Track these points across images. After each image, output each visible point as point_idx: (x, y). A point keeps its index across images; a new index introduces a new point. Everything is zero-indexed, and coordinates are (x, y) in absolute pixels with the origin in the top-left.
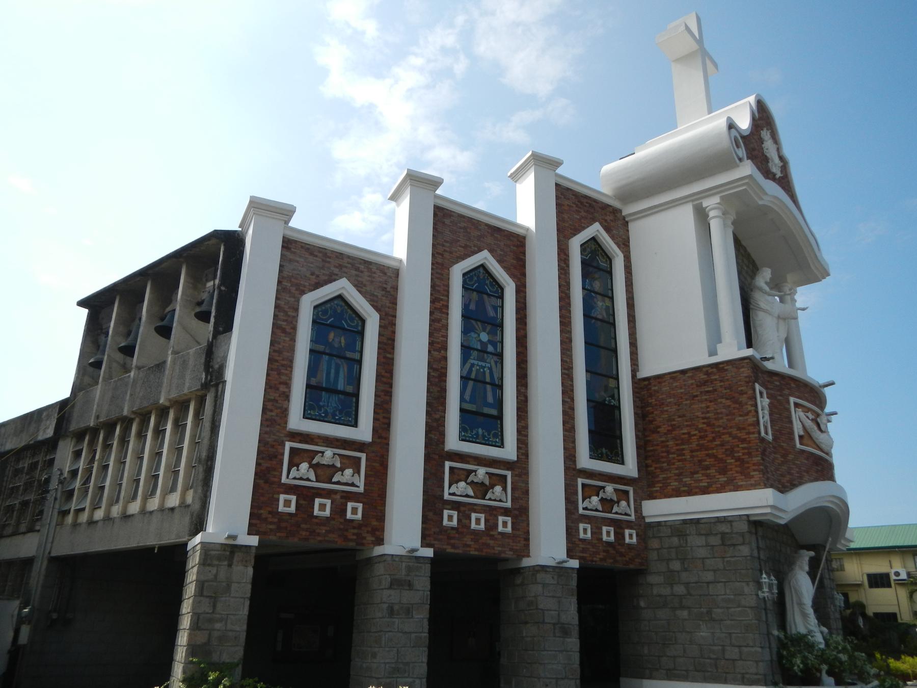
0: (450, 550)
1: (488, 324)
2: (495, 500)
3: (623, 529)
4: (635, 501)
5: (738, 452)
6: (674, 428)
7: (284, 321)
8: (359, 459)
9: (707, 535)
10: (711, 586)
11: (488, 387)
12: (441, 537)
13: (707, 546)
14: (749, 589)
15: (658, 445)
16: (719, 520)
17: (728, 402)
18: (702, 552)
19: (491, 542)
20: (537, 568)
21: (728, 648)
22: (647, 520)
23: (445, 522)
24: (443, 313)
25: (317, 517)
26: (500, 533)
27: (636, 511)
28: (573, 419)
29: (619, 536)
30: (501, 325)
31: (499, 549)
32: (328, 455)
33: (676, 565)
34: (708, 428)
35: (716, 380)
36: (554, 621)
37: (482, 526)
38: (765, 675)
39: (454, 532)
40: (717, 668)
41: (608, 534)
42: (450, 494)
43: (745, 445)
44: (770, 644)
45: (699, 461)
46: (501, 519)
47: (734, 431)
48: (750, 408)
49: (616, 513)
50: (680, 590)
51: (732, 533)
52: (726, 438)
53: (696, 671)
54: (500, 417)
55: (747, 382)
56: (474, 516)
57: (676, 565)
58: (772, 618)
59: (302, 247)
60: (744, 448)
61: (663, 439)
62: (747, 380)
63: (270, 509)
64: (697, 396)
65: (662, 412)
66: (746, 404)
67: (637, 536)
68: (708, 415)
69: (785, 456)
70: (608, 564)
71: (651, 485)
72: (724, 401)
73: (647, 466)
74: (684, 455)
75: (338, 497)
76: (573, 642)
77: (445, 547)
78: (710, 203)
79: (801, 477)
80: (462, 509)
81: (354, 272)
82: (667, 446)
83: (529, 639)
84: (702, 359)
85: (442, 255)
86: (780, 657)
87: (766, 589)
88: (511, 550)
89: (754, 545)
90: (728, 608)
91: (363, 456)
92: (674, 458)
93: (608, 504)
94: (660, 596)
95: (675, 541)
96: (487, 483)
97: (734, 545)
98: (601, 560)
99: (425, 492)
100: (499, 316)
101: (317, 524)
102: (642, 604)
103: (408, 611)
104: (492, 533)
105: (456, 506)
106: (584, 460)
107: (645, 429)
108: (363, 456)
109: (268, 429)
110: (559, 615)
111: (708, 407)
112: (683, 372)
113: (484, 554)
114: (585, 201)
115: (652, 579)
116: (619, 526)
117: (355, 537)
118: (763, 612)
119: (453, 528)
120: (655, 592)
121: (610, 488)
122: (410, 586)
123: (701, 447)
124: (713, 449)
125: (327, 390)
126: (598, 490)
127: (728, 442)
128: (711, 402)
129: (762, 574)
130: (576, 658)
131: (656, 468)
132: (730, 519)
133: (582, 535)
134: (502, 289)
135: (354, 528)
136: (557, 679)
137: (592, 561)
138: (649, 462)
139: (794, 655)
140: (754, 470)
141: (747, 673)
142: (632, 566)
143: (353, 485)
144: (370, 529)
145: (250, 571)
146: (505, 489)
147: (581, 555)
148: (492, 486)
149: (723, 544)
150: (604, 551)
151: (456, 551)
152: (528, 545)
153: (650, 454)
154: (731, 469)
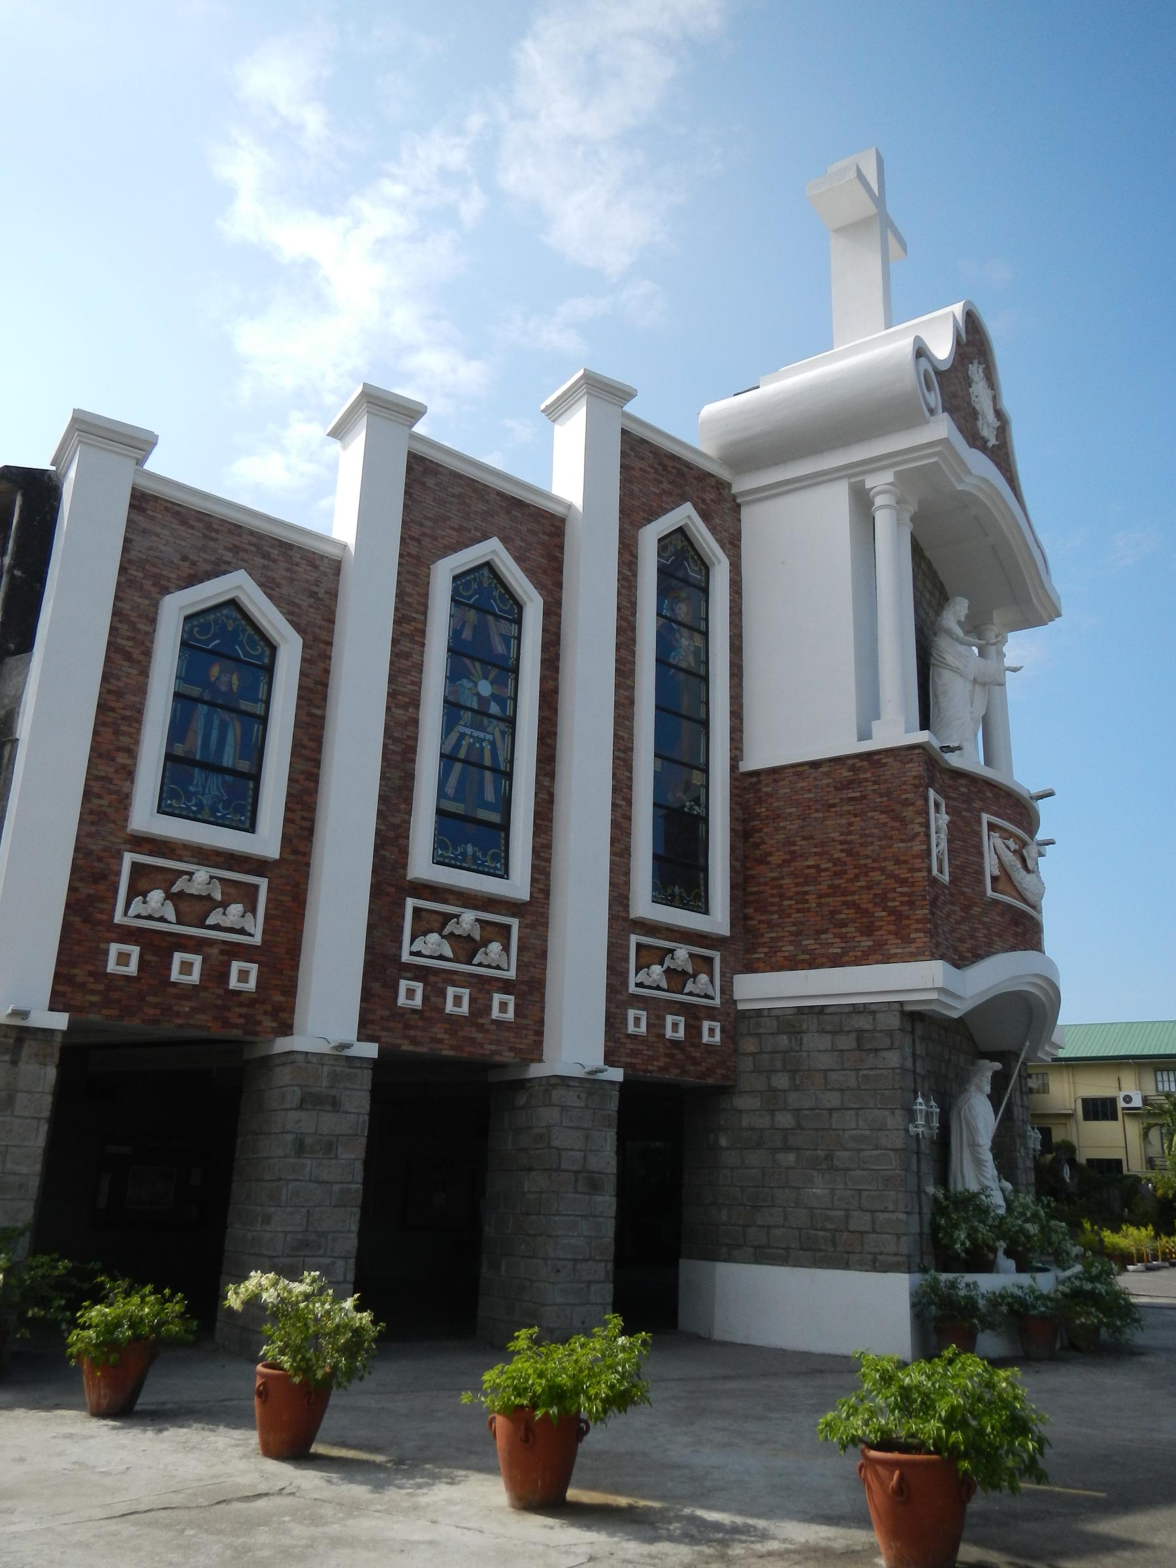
0: (406, 1047)
1: (494, 665)
2: (489, 966)
3: (699, 1019)
4: (723, 974)
5: (894, 900)
6: (793, 856)
7: (129, 639)
8: (256, 888)
9: (834, 1033)
10: (835, 1115)
11: (488, 775)
12: (392, 1024)
13: (833, 1050)
14: (895, 1120)
15: (765, 884)
16: (856, 1010)
17: (883, 818)
18: (825, 1061)
19: (479, 1036)
20: (553, 1081)
21: (856, 1214)
22: (741, 1007)
23: (402, 1000)
24: (416, 643)
25: (175, 984)
26: (494, 1022)
27: (723, 992)
28: (629, 834)
29: (693, 1030)
30: (515, 670)
31: (493, 1047)
32: (201, 879)
33: (781, 1081)
34: (848, 859)
35: (866, 780)
36: (575, 1168)
37: (465, 1009)
38: (909, 1256)
39: (416, 1017)
40: (834, 1245)
41: (674, 1028)
42: (412, 954)
43: (905, 890)
44: (920, 1207)
45: (833, 913)
46: (497, 998)
47: (890, 866)
48: (918, 829)
49: (690, 994)
50: (785, 1120)
51: (874, 1030)
52: (876, 876)
53: (802, 1249)
54: (504, 827)
55: (916, 786)
56: (451, 991)
57: (781, 1081)
58: (927, 1167)
59: (167, 509)
60: (902, 894)
61: (774, 875)
62: (917, 782)
63: (91, 968)
64: (834, 805)
65: (777, 829)
66: (912, 822)
67: (722, 1031)
68: (849, 838)
69: (966, 908)
70: (672, 1075)
71: (751, 949)
72: (876, 815)
73: (746, 918)
74: (807, 901)
75: (215, 951)
76: (607, 1202)
77: (398, 1041)
78: (878, 481)
79: (990, 944)
80: (432, 979)
81: (260, 561)
82: (781, 887)
83: (531, 1196)
84: (847, 744)
85: (419, 541)
86: (935, 1228)
87: (921, 1121)
88: (511, 1049)
89: (908, 1051)
90: (859, 1151)
91: (263, 883)
92: (790, 906)
93: (677, 978)
94: (752, 1129)
95: (783, 1041)
96: (478, 938)
97: (876, 1050)
98: (660, 1069)
99: (369, 948)
100: (513, 654)
101: (176, 996)
102: (723, 1142)
103: (329, 1147)
104: (480, 1021)
105: (420, 973)
106: (644, 905)
107: (746, 857)
108: (263, 883)
109: (93, 829)
110: (585, 1158)
111: (851, 824)
112: (815, 764)
113: (465, 1055)
114: (670, 463)
115: (741, 1102)
116: (693, 1015)
117: (242, 1021)
118: (915, 1156)
119: (414, 1011)
120: (745, 1124)
121: (682, 953)
122: (335, 1104)
123: (835, 890)
124: (854, 893)
125: (205, 766)
126: (662, 955)
127: (879, 883)
128: (856, 816)
129: (916, 1098)
130: (609, 1229)
131: (760, 922)
132: (873, 1008)
133: (631, 1029)
134: (520, 608)
135: (241, 1005)
136: (575, 1261)
137: (646, 1071)
138: (750, 911)
139: (956, 1226)
140: (917, 930)
141: (881, 1253)
142: (710, 1081)
143: (242, 931)
144: (269, 1008)
145: (51, 1073)
146: (506, 948)
147: (628, 1060)
148: (485, 943)
149: (860, 1048)
150: (666, 1055)
151: (419, 1049)
152: (541, 1042)
153: (752, 898)
154: (880, 928)
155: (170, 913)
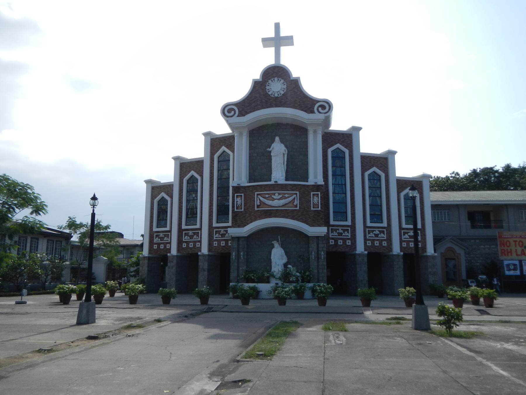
32: (161, 235)
41: (223, 244)
70: (223, 251)
76: (206, 273)
105: (186, 242)
121: (222, 230)
122: (172, 262)
133: (214, 245)
155: (159, 240)
